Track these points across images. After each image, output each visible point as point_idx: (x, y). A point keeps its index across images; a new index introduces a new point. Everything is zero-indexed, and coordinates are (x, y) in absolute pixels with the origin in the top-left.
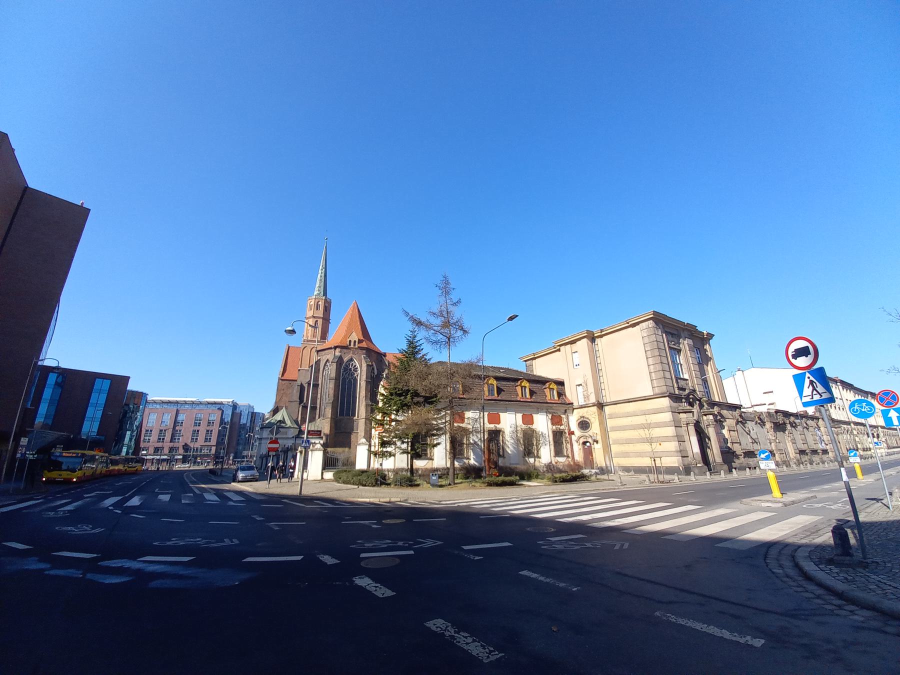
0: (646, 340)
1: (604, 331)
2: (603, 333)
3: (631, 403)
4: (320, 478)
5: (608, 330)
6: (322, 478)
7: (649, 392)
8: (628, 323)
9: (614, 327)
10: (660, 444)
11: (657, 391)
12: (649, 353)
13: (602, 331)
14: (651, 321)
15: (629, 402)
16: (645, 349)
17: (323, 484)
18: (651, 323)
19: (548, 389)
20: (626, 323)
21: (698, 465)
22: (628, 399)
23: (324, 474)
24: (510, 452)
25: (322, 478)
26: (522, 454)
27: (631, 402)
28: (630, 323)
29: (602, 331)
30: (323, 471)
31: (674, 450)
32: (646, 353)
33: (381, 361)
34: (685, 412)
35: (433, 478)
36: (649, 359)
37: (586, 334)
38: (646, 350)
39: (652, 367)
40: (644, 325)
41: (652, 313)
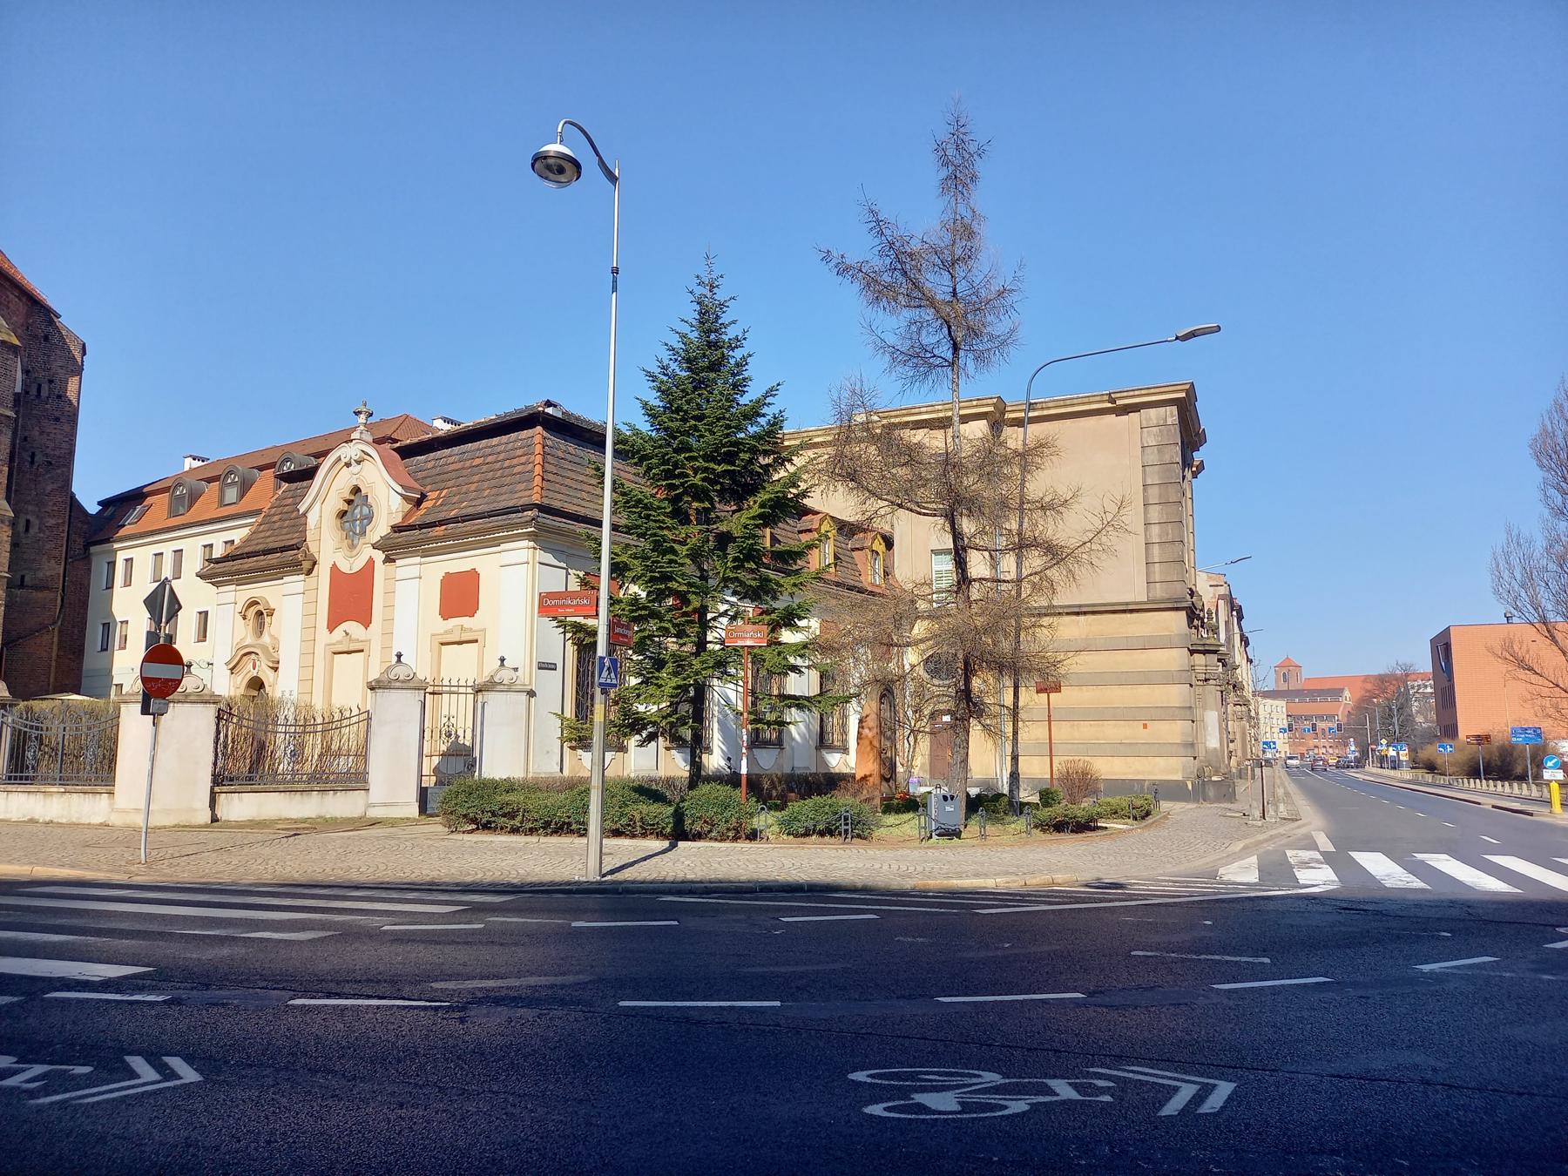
0: (1153, 457)
1: (1034, 410)
2: (1031, 414)
3: (1082, 618)
4: (205, 817)
5: (1048, 408)
6: (215, 819)
7: (1138, 594)
8: (1113, 401)
9: (1068, 402)
10: (1145, 726)
11: (1159, 592)
12: (1154, 492)
13: (1031, 407)
14: (1175, 408)
15: (1078, 614)
16: (1144, 479)
17: (217, 837)
18: (1171, 414)
19: (869, 554)
20: (1106, 398)
21: (1214, 778)
22: (1080, 606)
23: (222, 798)
24: (797, 737)
25: (215, 819)
26: (813, 743)
27: (1085, 613)
28: (1118, 402)
29: (1031, 407)
30: (217, 789)
31: (1178, 741)
32: (1145, 490)
33: (46, 338)
34: (1204, 652)
35: (948, 809)
36: (1151, 507)
37: (992, 409)
38: (1149, 482)
39: (1155, 530)
40: (1152, 412)
41: (1187, 387)
